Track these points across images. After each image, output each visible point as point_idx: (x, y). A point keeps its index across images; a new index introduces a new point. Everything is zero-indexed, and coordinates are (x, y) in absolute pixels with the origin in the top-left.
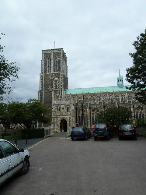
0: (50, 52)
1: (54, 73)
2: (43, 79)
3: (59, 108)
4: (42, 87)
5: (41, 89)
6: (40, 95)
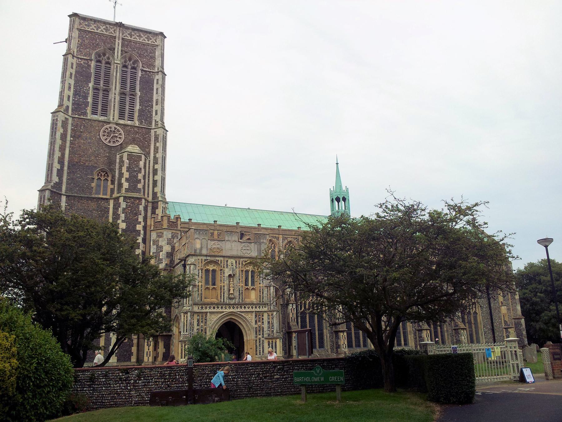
1: (121, 122)
2: (69, 138)
3: (214, 271)
4: (60, 173)
5: (55, 179)
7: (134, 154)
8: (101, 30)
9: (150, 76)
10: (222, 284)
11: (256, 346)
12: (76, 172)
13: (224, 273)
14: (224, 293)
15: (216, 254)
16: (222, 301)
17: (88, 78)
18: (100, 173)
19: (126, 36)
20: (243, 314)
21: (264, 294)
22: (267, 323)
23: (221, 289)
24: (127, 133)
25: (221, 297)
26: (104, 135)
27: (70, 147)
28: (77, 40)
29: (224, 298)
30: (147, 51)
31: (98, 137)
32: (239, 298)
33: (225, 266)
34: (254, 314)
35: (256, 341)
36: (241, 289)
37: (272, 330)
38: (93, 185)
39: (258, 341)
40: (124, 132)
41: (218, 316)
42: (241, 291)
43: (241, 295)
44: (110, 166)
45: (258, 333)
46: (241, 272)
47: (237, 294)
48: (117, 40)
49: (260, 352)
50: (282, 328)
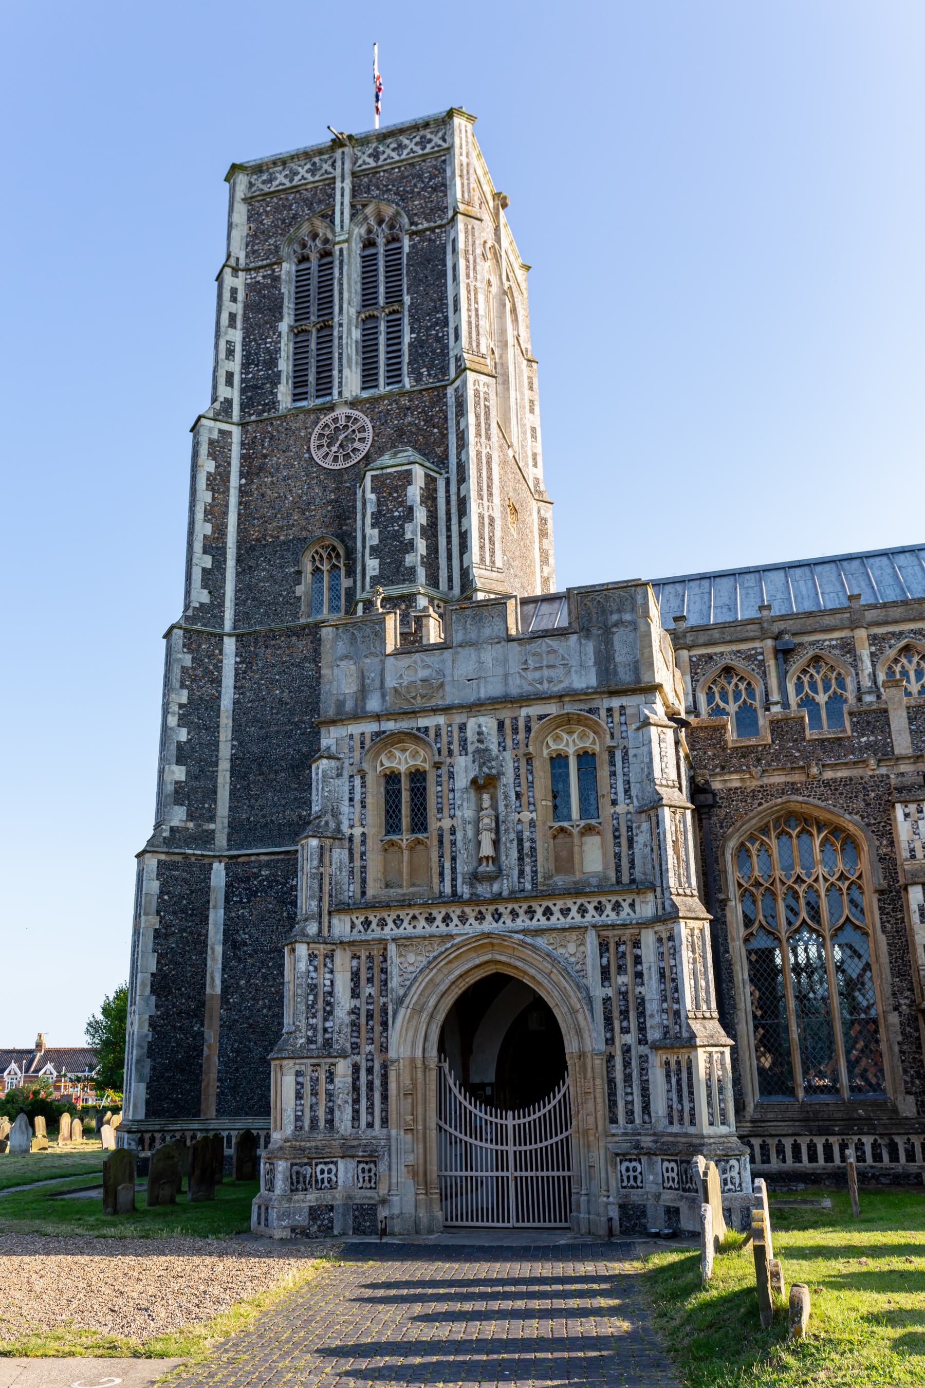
0: (313, 172)
1: (366, 395)
2: (235, 481)
3: (418, 777)
5: (202, 596)
6: (189, 678)
7: (389, 470)
8: (299, 177)
9: (434, 241)
10: (446, 824)
11: (611, 1082)
12: (257, 565)
13: (451, 776)
14: (454, 859)
15: (419, 703)
17: (276, 311)
18: (317, 552)
19: (364, 163)
21: (637, 848)
22: (655, 977)
23: (441, 842)
24: (380, 420)
25: (441, 874)
26: (320, 447)
27: (240, 503)
28: (246, 228)
29: (454, 879)
30: (420, 177)
31: (307, 455)
32: (521, 873)
33: (455, 747)
34: (592, 939)
35: (610, 1058)
36: (526, 834)
37: (676, 1006)
38: (300, 590)
40: (372, 420)
42: (527, 845)
43: (527, 860)
44: (340, 526)
45: (617, 1024)
46: (523, 762)
47: (510, 858)
48: (338, 185)
49: (630, 1113)
50: (894, 994)
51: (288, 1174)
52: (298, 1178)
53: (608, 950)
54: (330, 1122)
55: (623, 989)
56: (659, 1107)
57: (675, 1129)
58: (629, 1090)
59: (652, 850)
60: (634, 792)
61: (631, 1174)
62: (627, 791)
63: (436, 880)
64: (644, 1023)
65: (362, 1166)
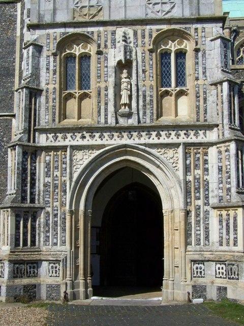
3: (85, 57)
10: (103, 85)
13: (106, 59)
16: (103, 120)
20: (154, 151)
21: (209, 103)
22: (216, 170)
25: (99, 112)
29: (106, 115)
33: (109, 44)
34: (180, 150)
36: (148, 93)
39: (193, 213)
41: (93, 156)
42: (148, 99)
43: (148, 107)
46: (148, 53)
51: (12, 268)
52: (17, 271)
53: (190, 156)
54: (33, 243)
55: (198, 177)
56: (214, 236)
57: (224, 248)
58: (198, 228)
59: (217, 104)
60: (208, 74)
61: (199, 270)
62: (204, 73)
63: (95, 114)
64: (208, 194)
65: (51, 265)
